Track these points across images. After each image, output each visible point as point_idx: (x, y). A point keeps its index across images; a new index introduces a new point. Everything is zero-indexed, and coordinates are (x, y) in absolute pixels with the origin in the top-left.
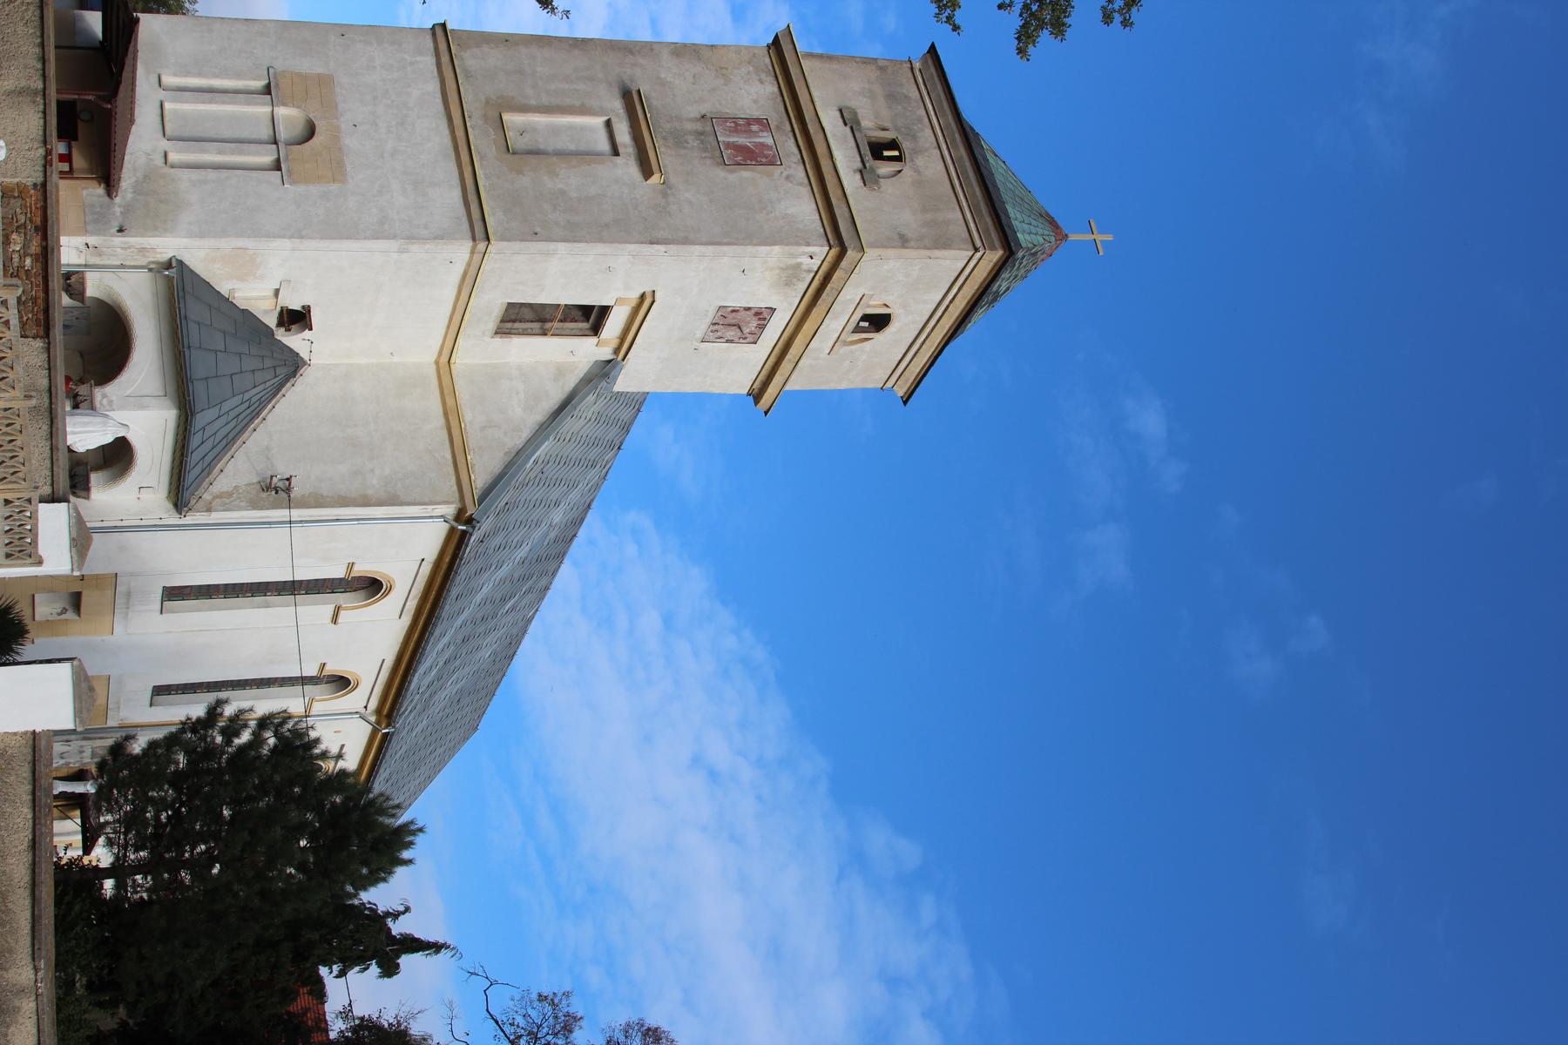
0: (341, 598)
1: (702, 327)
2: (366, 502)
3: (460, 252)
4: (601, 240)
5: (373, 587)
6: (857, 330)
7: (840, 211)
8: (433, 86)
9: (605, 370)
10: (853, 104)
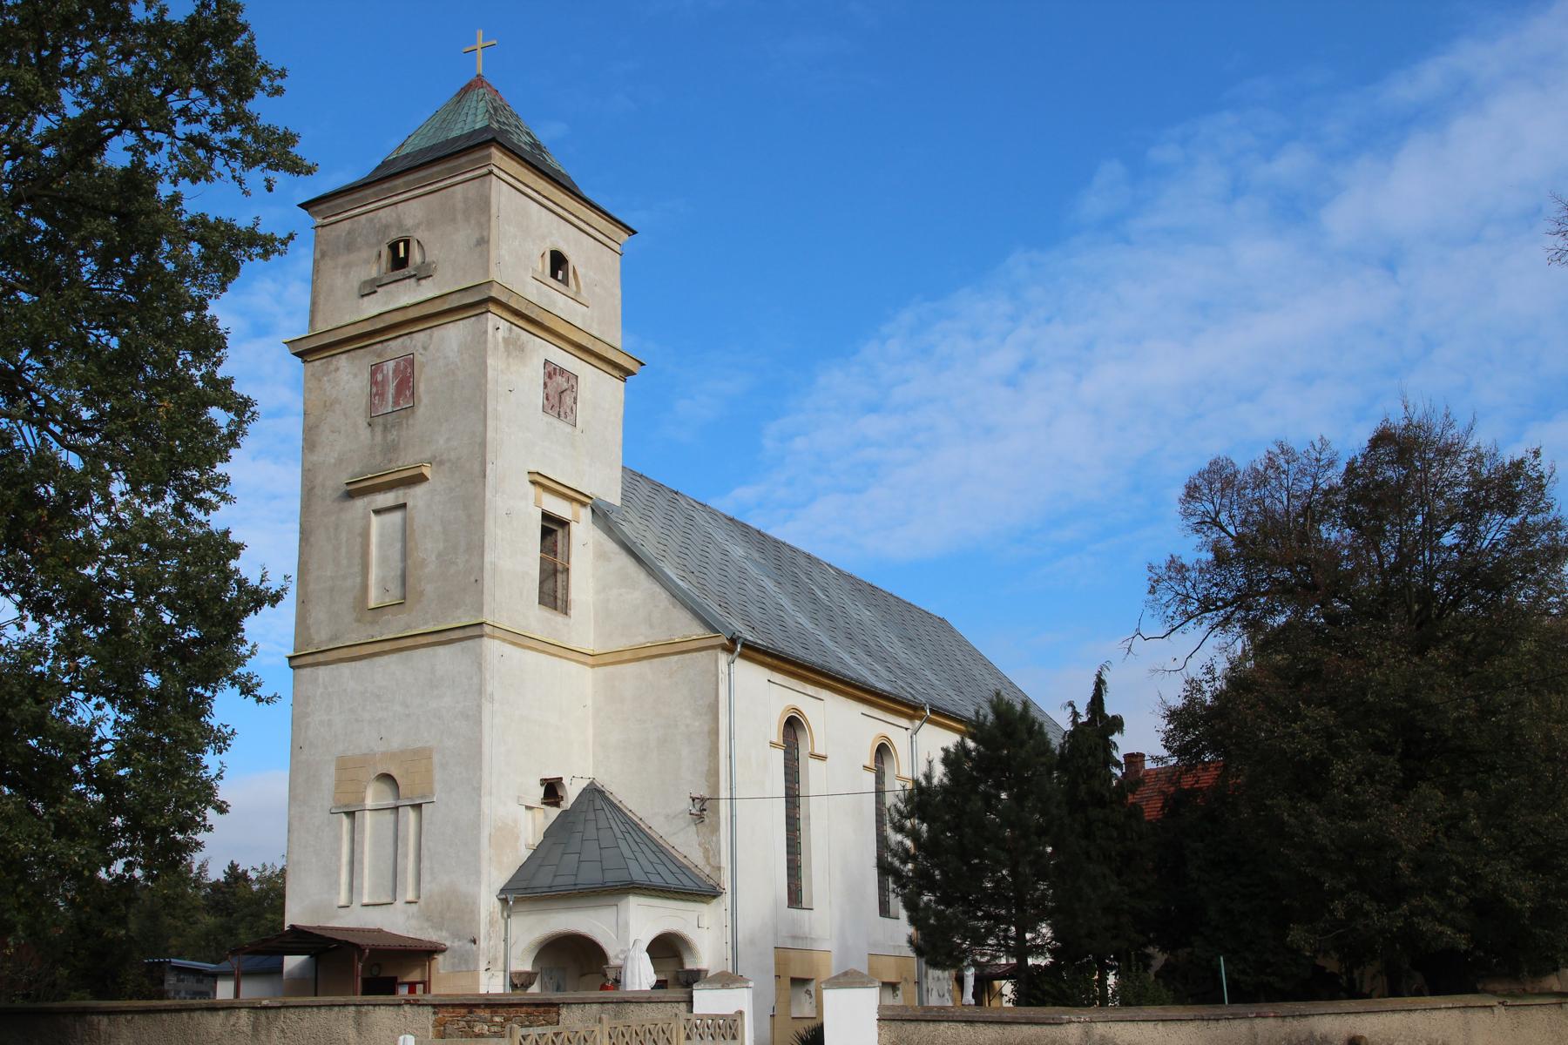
0: (803, 752)
1: (562, 427)
2: (715, 732)
3: (493, 648)
4: (482, 522)
5: (793, 725)
6: (565, 282)
8: (345, 668)
9: (601, 514)
10: (356, 285)
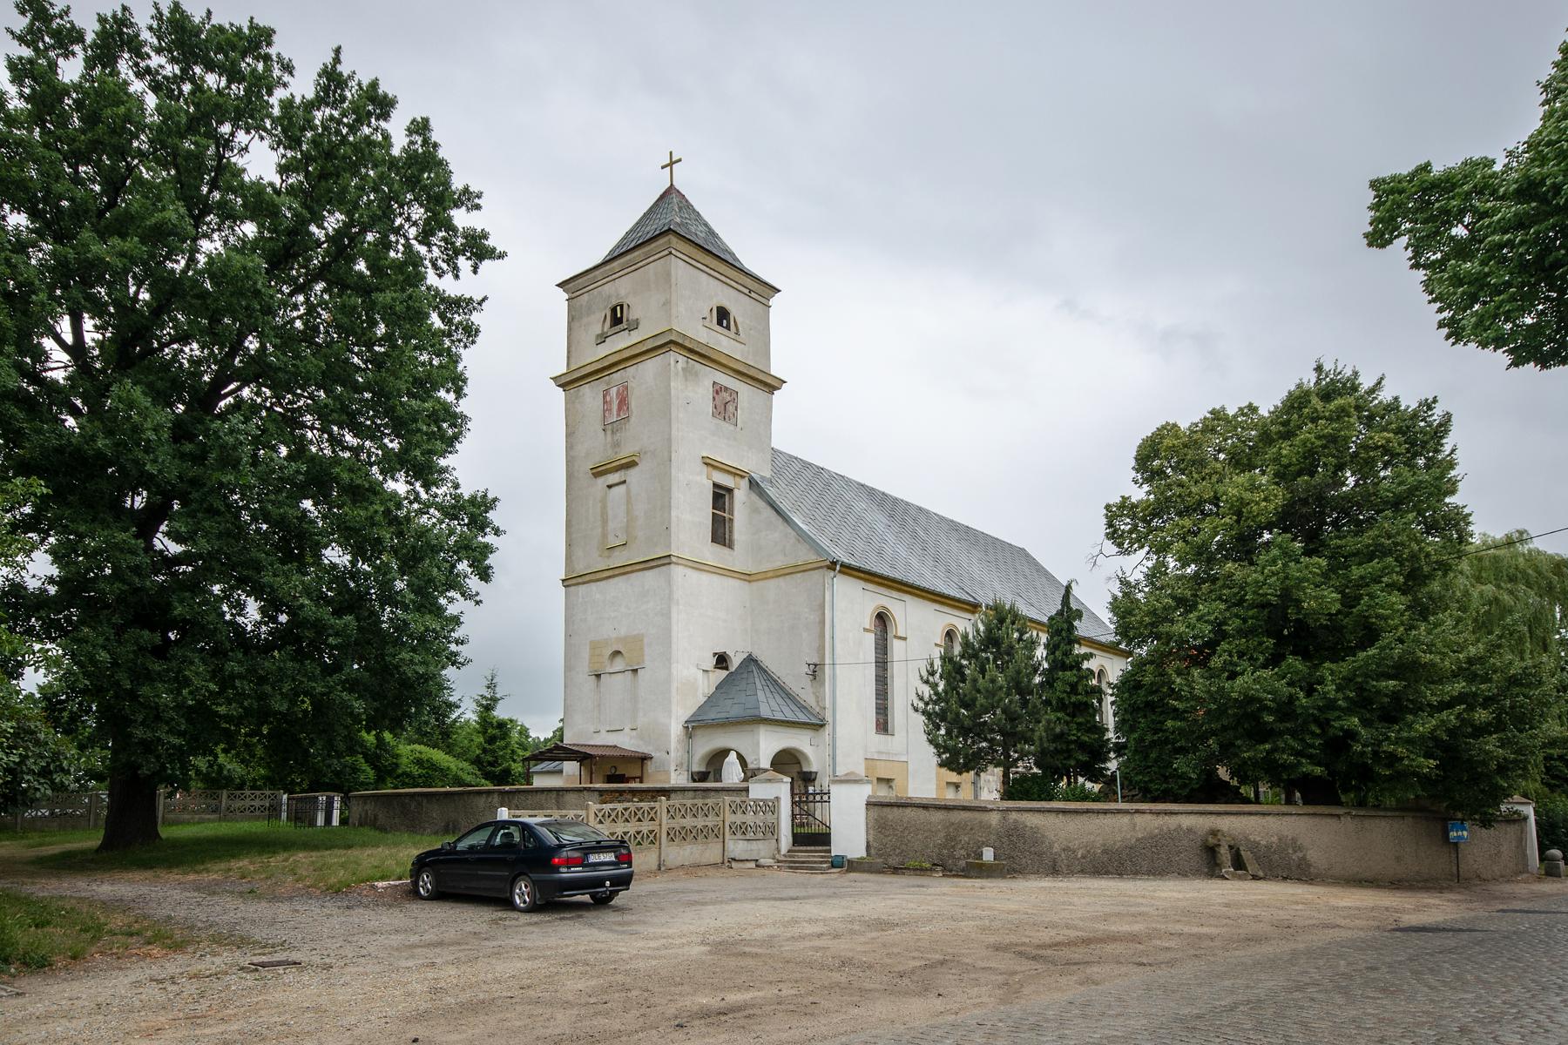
0: (890, 635)
1: (727, 427)
2: (823, 622)
3: (678, 572)
4: (670, 490)
5: (882, 618)
6: (728, 328)
7: (650, 345)
8: (593, 586)
9: (753, 485)
10: (594, 338)
